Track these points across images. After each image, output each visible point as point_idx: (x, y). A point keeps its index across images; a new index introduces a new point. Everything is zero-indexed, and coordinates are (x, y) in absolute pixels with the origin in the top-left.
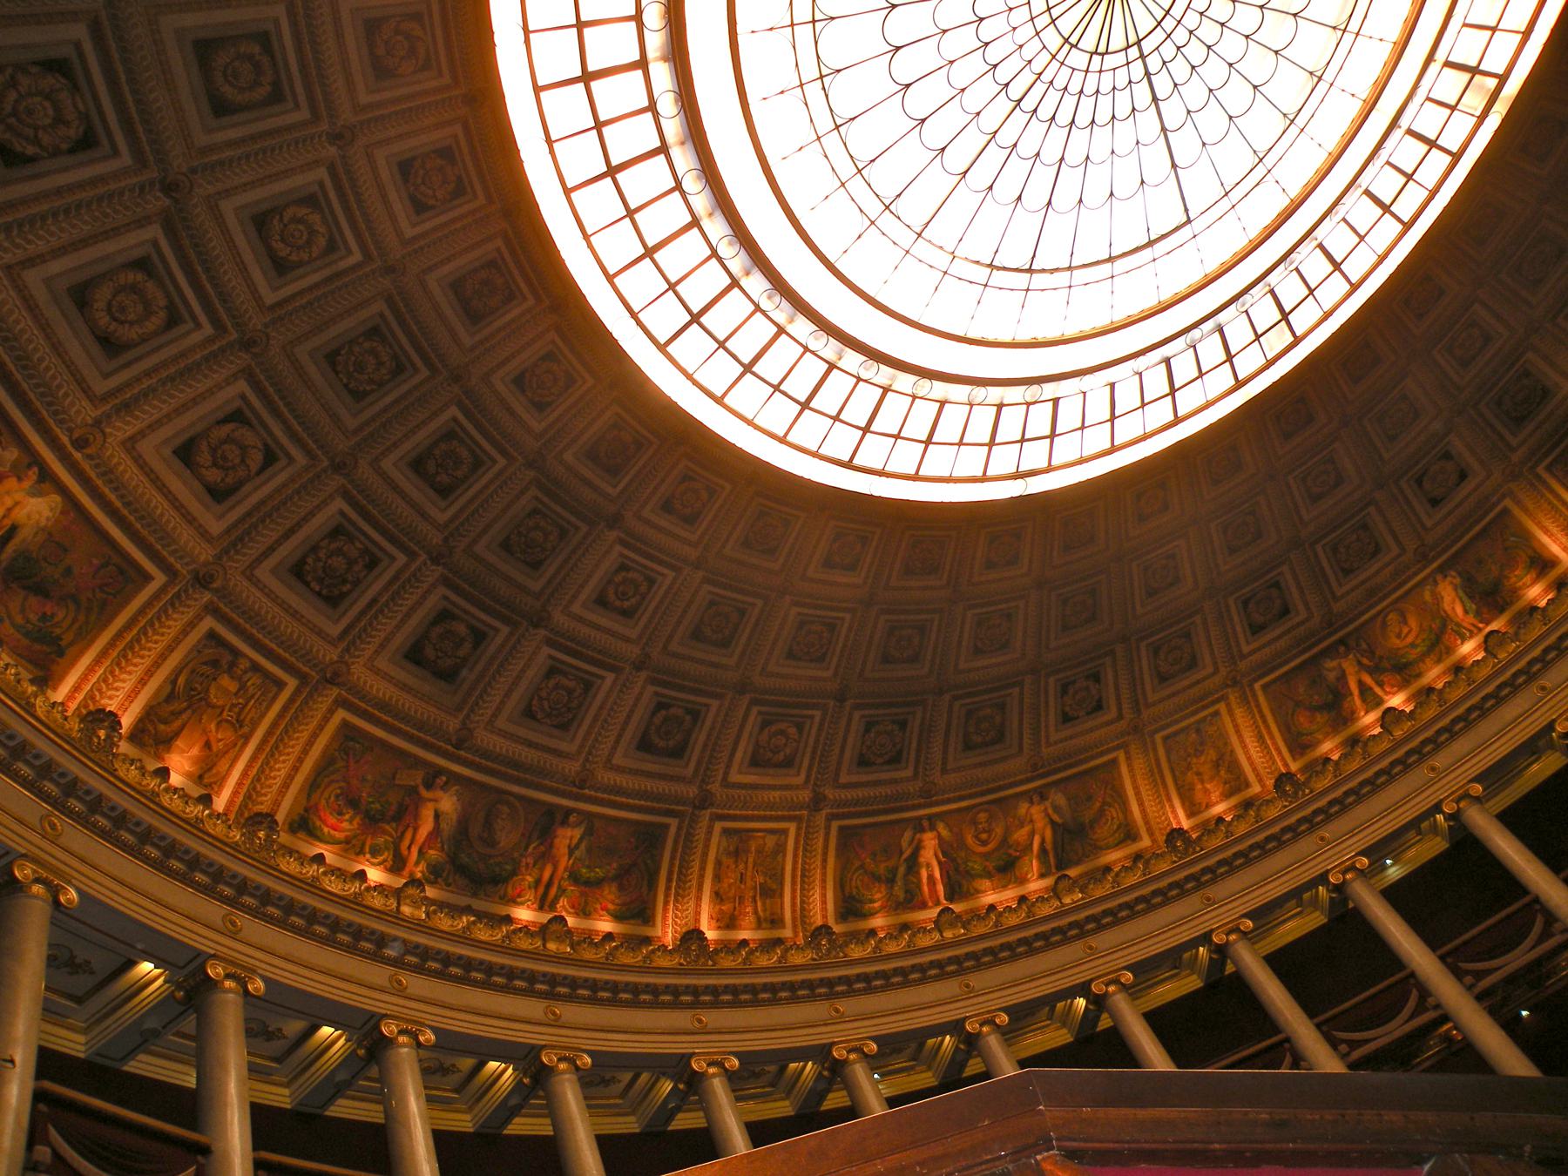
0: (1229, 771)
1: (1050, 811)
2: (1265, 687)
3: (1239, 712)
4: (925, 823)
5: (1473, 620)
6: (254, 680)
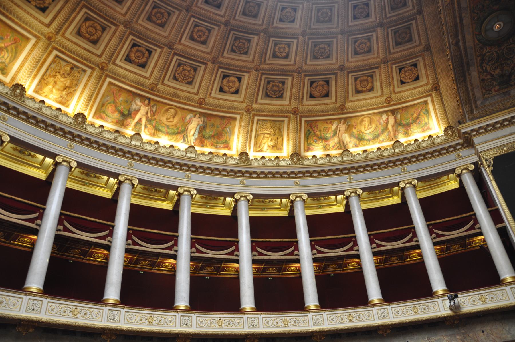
0: (67, 94)
3: (92, 80)
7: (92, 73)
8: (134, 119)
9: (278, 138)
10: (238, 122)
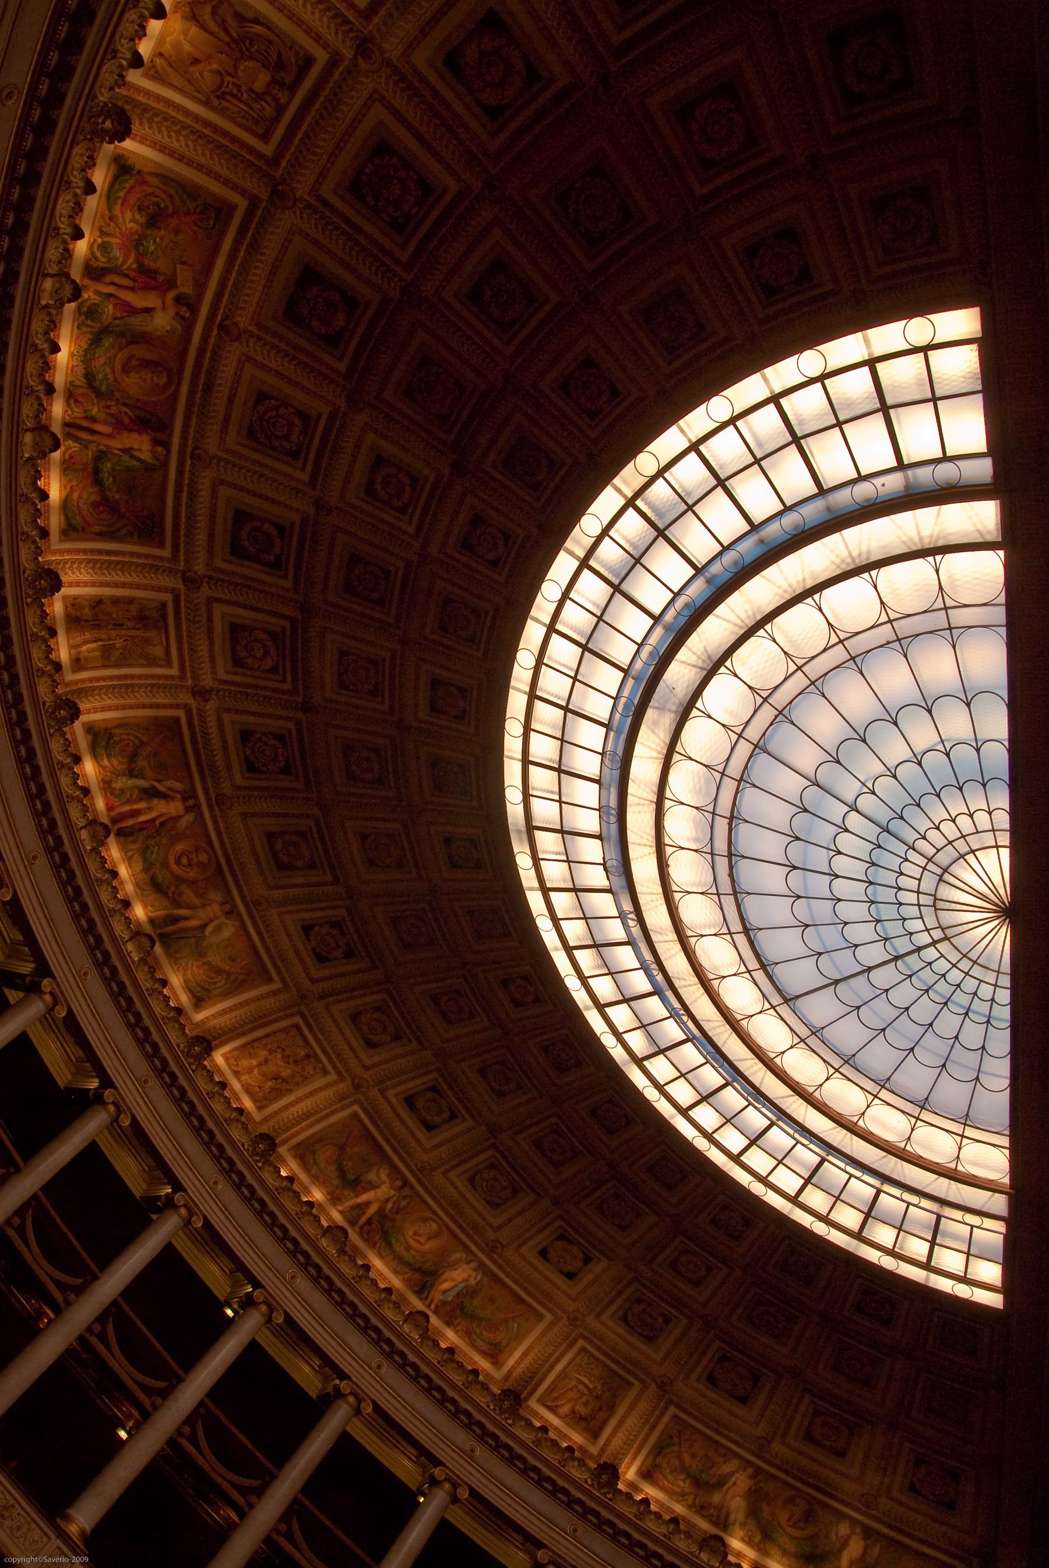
0: (272, 1089)
1: (215, 923)
2: (355, 1115)
3: (329, 1093)
4: (191, 802)
5: (436, 1301)
6: (269, 111)
7: (335, 1082)
8: (357, 1196)
9: (600, 1409)
10: (541, 1327)
